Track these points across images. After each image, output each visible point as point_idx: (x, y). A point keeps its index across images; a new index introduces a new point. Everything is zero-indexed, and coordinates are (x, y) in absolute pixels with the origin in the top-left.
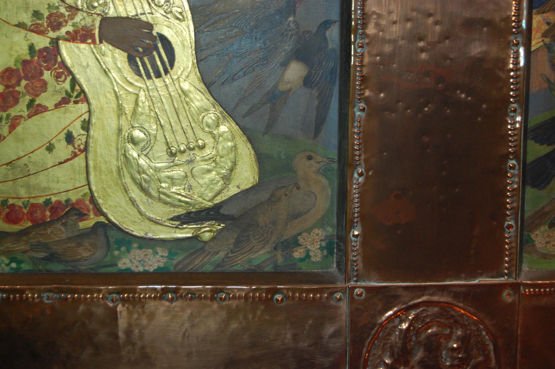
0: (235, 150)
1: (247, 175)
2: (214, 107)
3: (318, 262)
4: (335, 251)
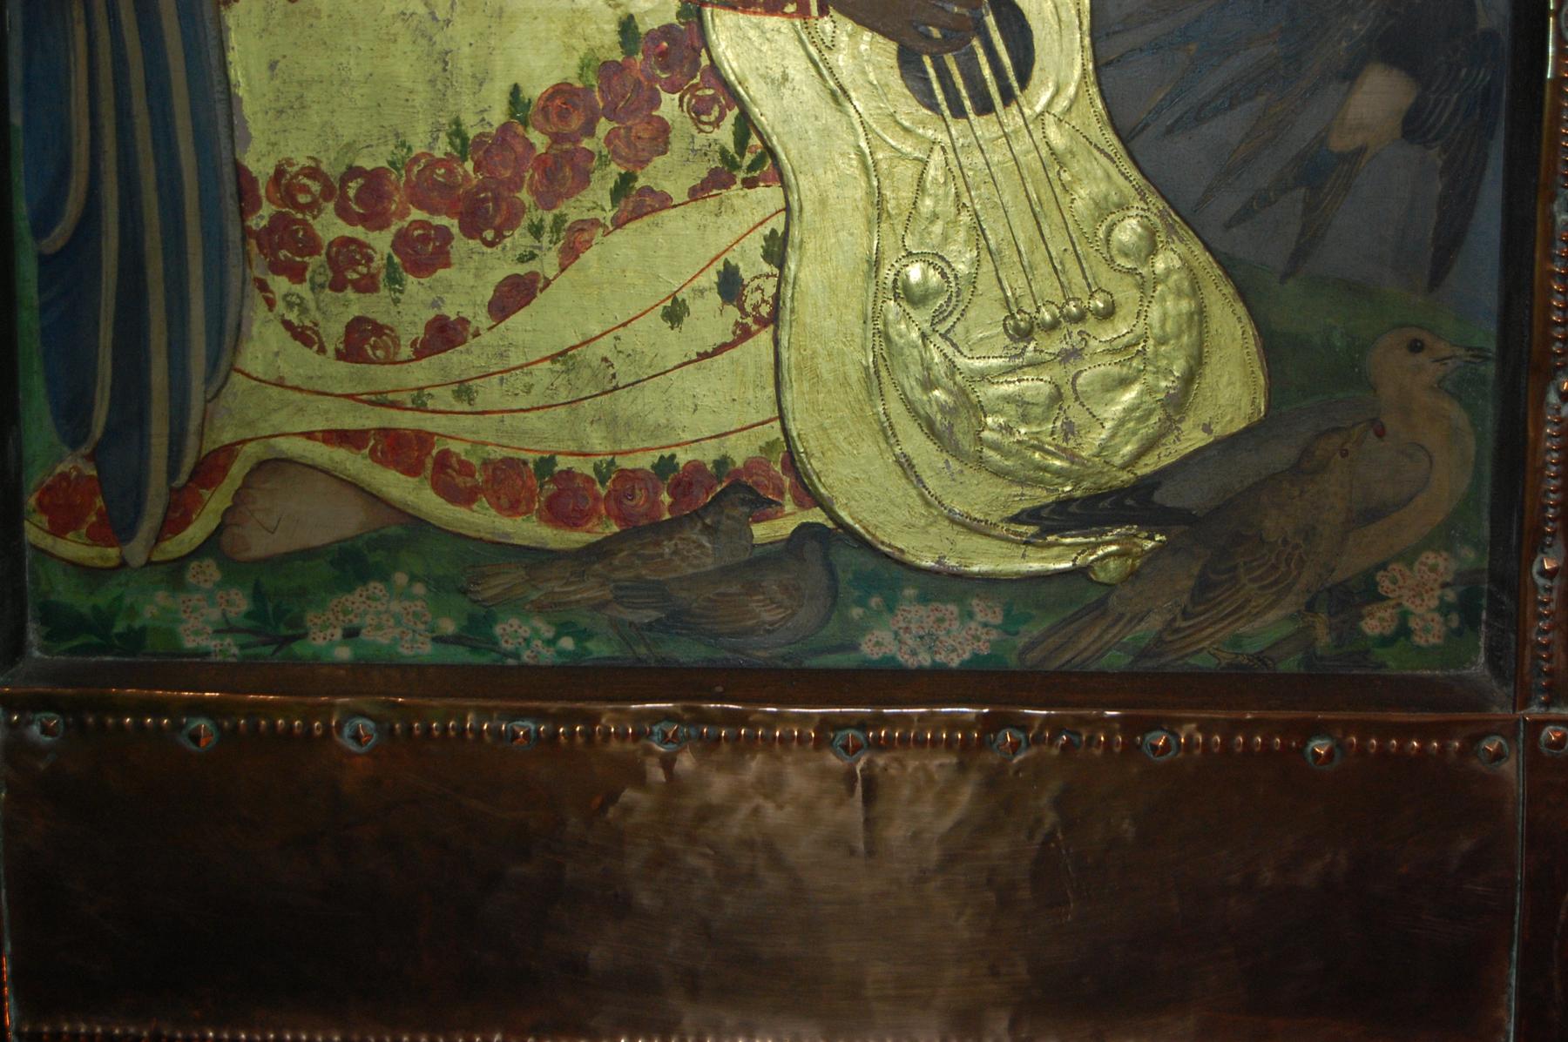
0: (1201, 322)
1: (1233, 395)
2: (1143, 199)
3: (1435, 647)
4: (1484, 616)
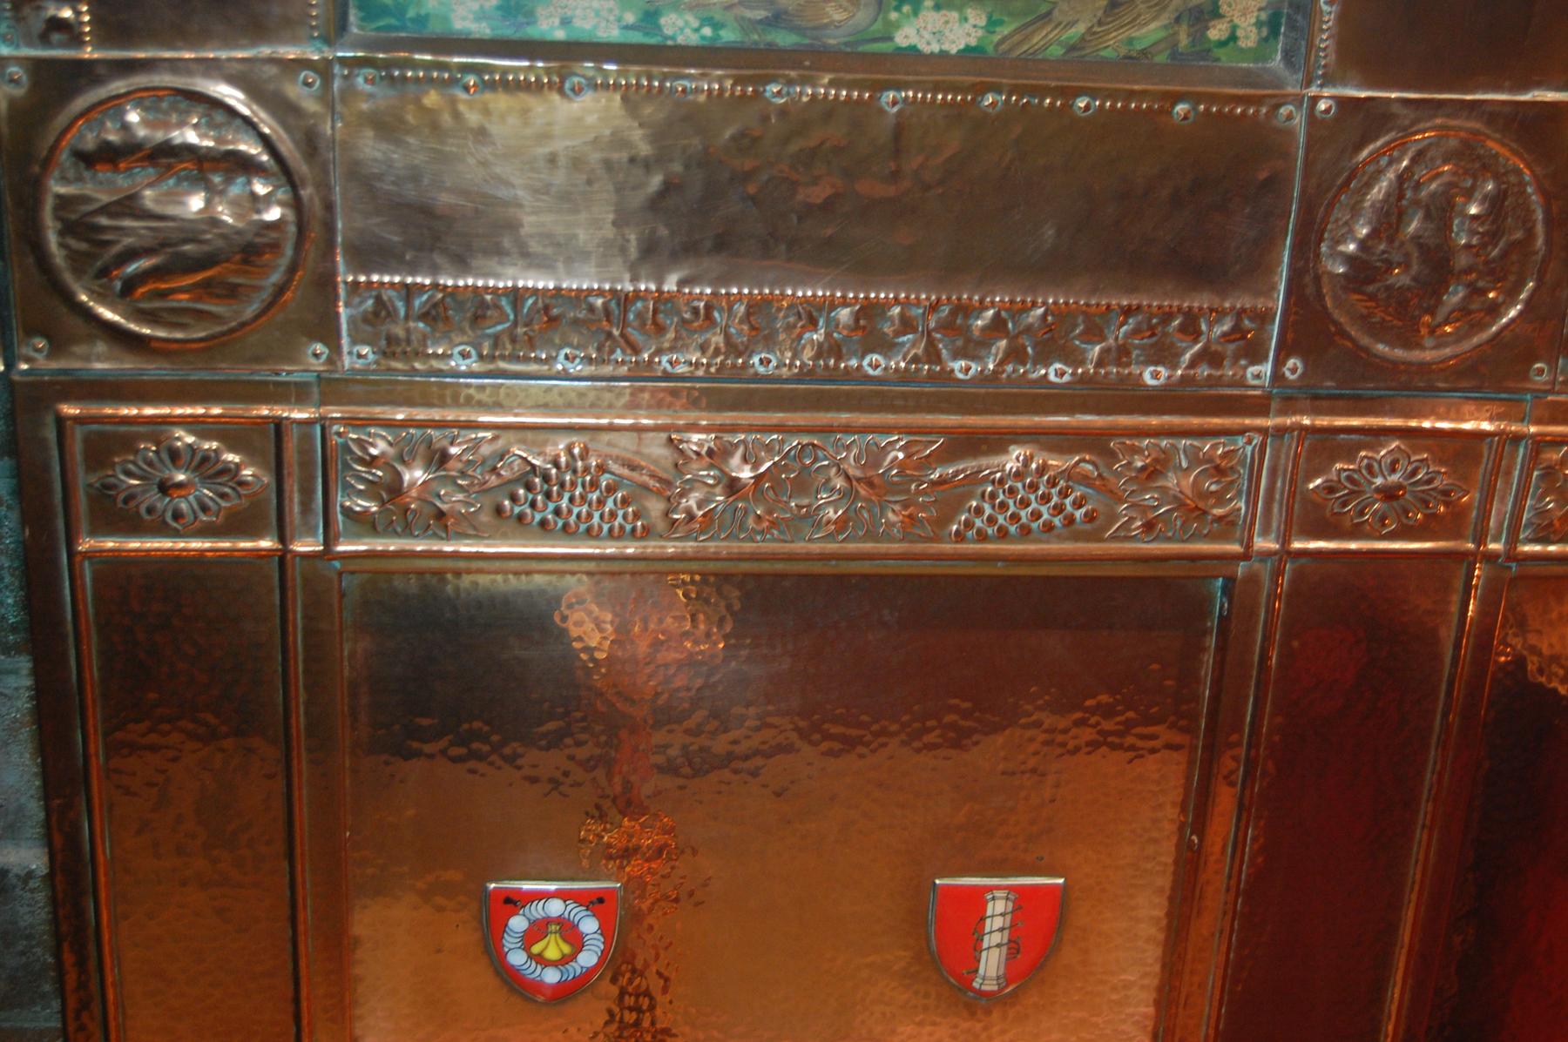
3: (1250, 49)
